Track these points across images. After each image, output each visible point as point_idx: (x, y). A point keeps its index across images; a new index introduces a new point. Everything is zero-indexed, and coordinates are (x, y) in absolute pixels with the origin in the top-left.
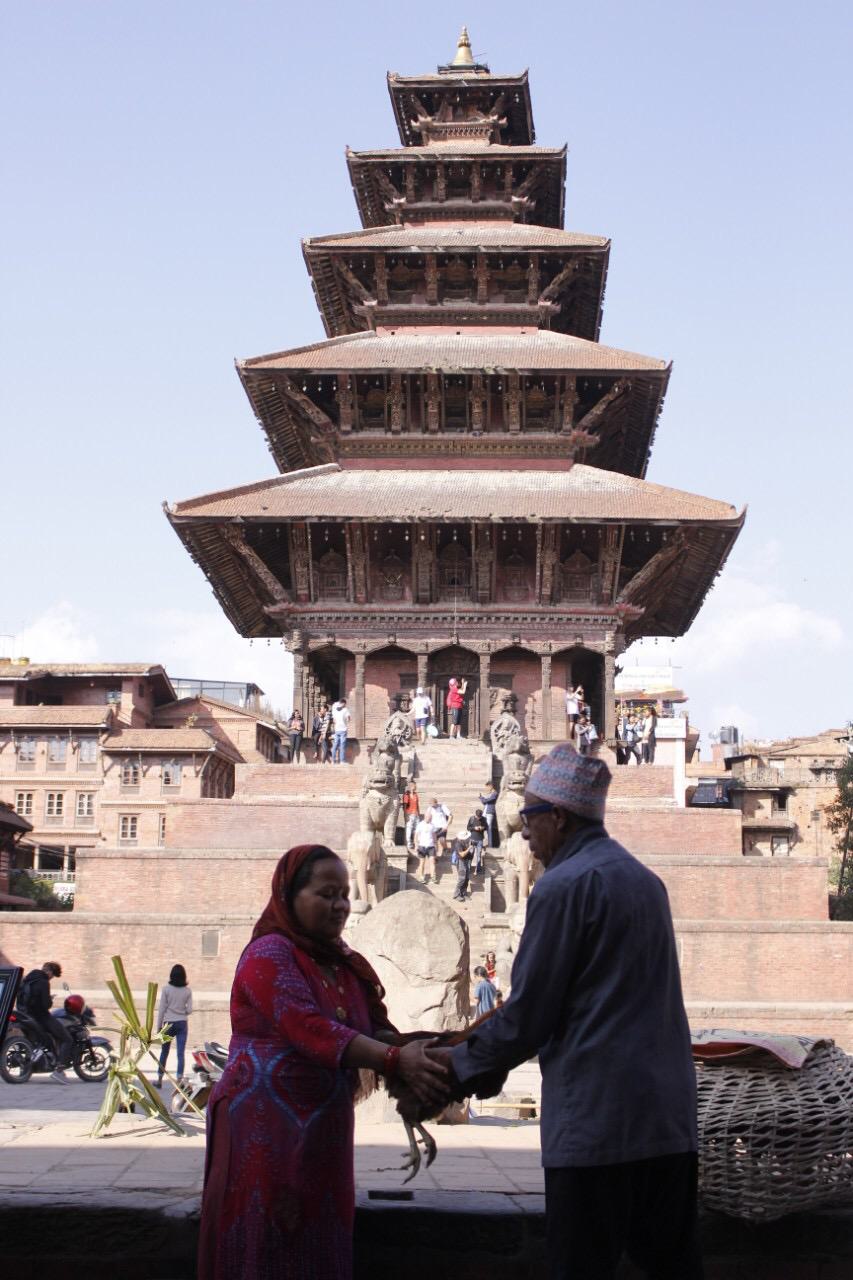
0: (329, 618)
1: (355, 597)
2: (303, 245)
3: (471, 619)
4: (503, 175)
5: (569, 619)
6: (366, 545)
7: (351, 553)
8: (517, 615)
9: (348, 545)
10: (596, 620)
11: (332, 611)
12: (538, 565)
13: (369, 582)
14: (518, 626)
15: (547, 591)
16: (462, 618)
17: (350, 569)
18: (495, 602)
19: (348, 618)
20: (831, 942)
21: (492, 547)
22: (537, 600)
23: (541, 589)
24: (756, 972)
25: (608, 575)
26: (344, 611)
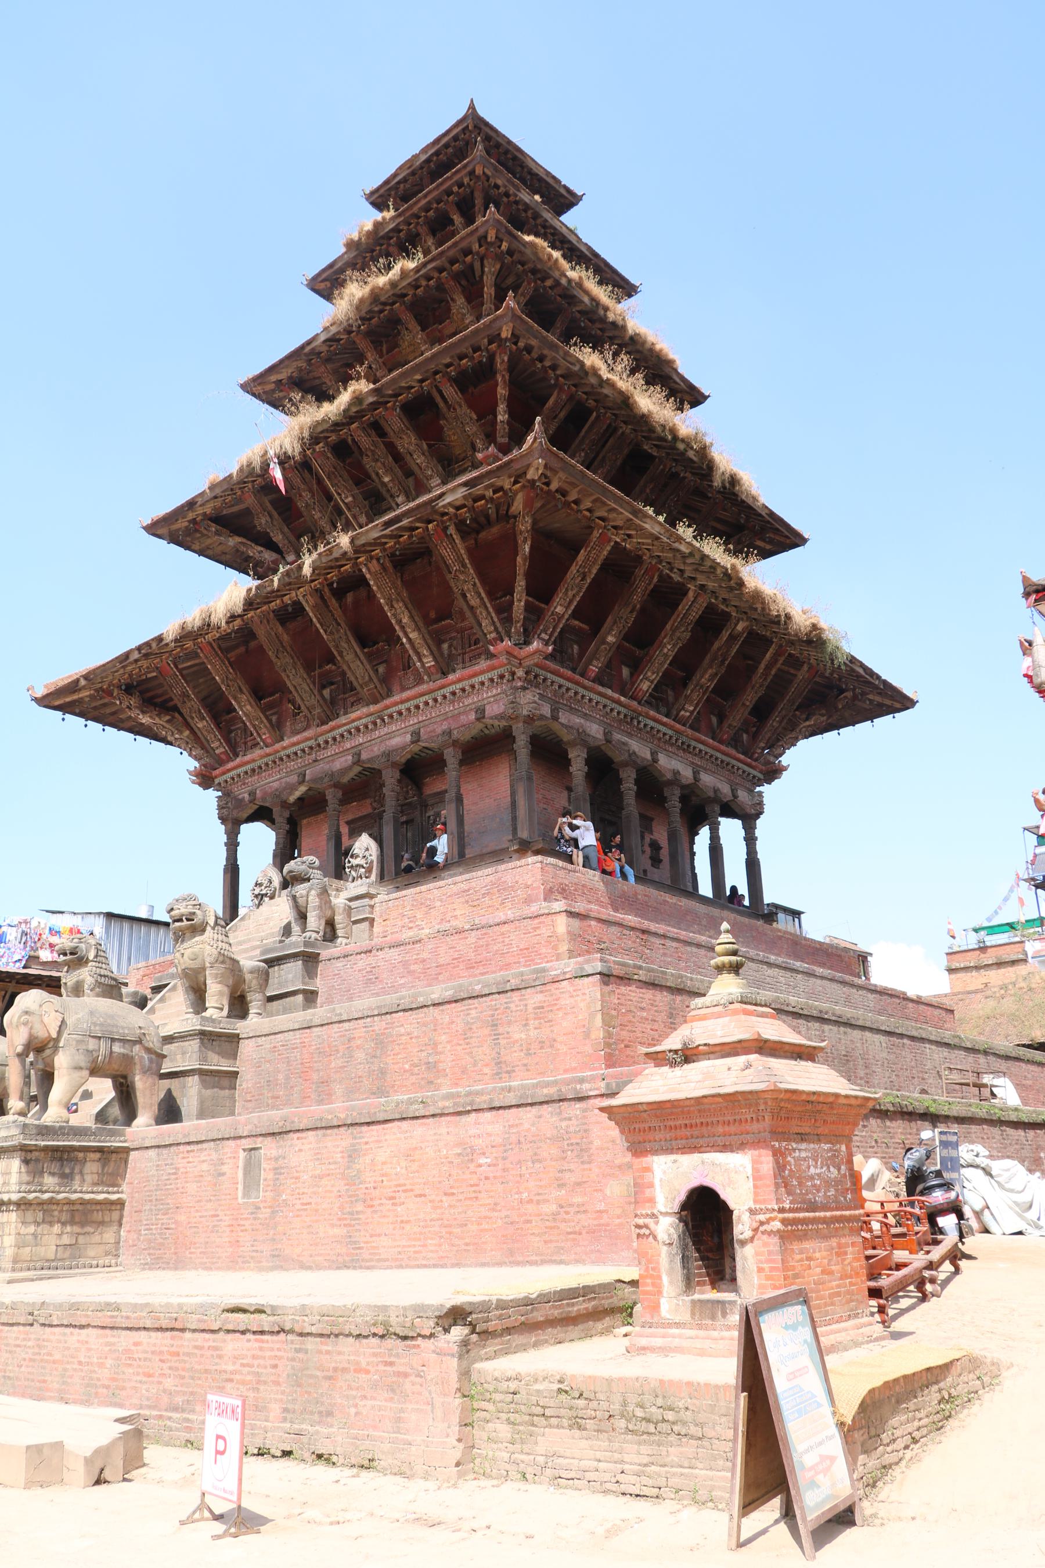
0: (246, 773)
1: (263, 741)
4: (452, 222)
5: (463, 690)
10: (492, 680)
15: (429, 662)
16: (358, 729)
18: (388, 696)
19: (260, 767)
20: (473, 1131)
21: (339, 624)
22: (426, 678)
23: (420, 660)
24: (360, 1207)
25: (481, 613)
26: (254, 761)
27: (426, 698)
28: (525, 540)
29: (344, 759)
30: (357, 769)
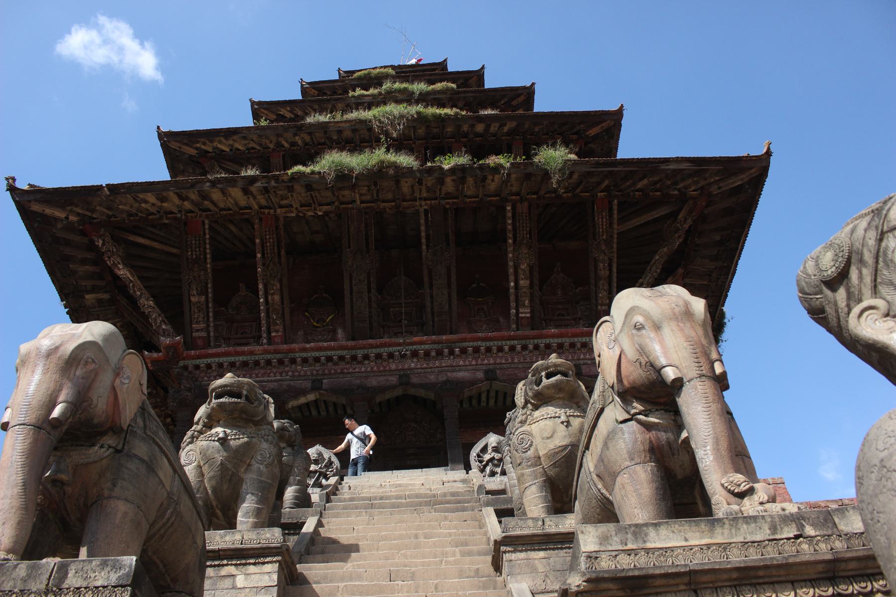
1: (269, 338)
2: (253, 103)
3: (427, 354)
6: (283, 253)
7: (264, 265)
8: (488, 344)
9: (259, 255)
11: (238, 354)
12: (511, 270)
13: (287, 311)
14: (492, 361)
15: (525, 313)
17: (261, 293)
19: (257, 363)
22: (514, 326)
23: (517, 309)
26: (252, 353)
27: (516, 342)
28: (679, 237)
29: (383, 378)
30: (398, 392)
